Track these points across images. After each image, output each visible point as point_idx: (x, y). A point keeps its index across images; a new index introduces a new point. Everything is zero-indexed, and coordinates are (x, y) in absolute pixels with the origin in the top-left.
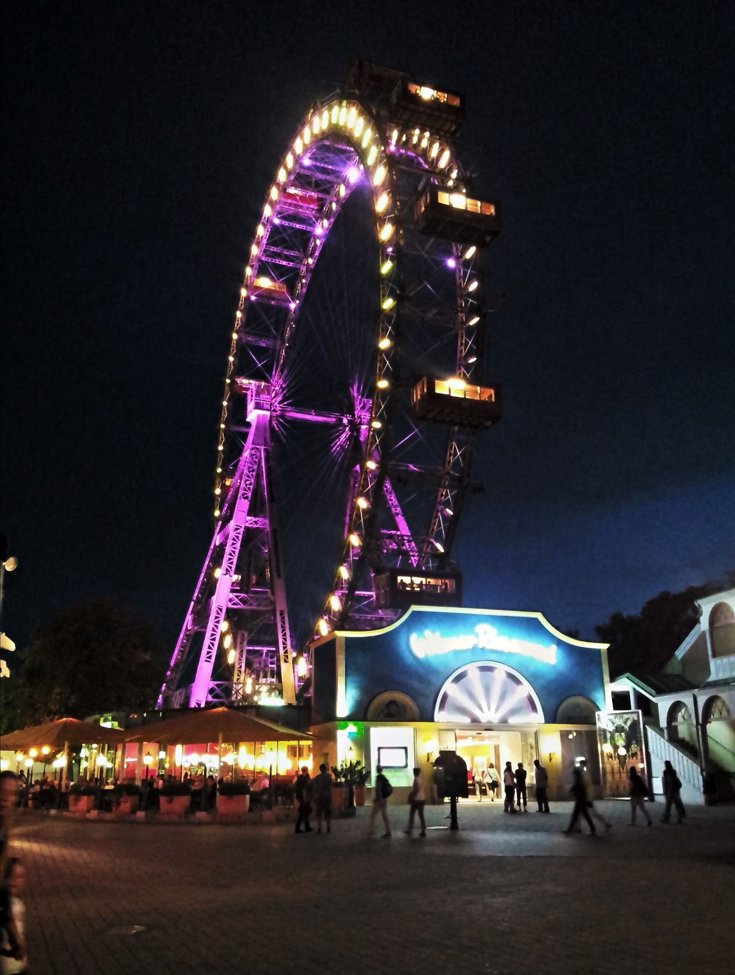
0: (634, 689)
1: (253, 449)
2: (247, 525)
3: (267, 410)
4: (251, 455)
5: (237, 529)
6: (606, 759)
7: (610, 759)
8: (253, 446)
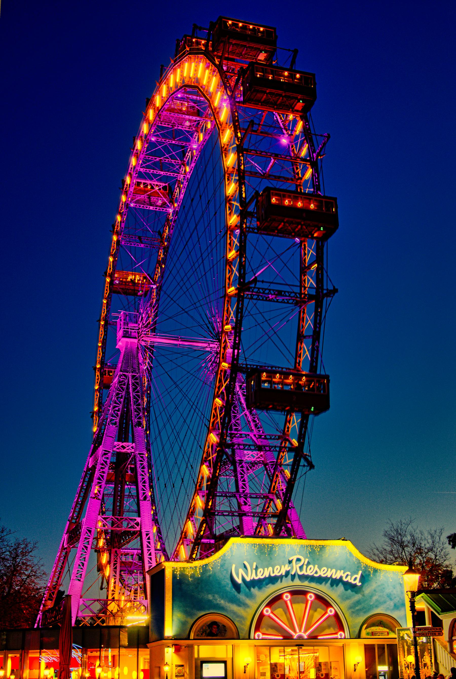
0: (429, 609)
1: (121, 376)
2: (115, 449)
3: (136, 338)
4: (119, 382)
5: (105, 454)
6: (404, 668)
7: (407, 669)
8: (121, 373)
